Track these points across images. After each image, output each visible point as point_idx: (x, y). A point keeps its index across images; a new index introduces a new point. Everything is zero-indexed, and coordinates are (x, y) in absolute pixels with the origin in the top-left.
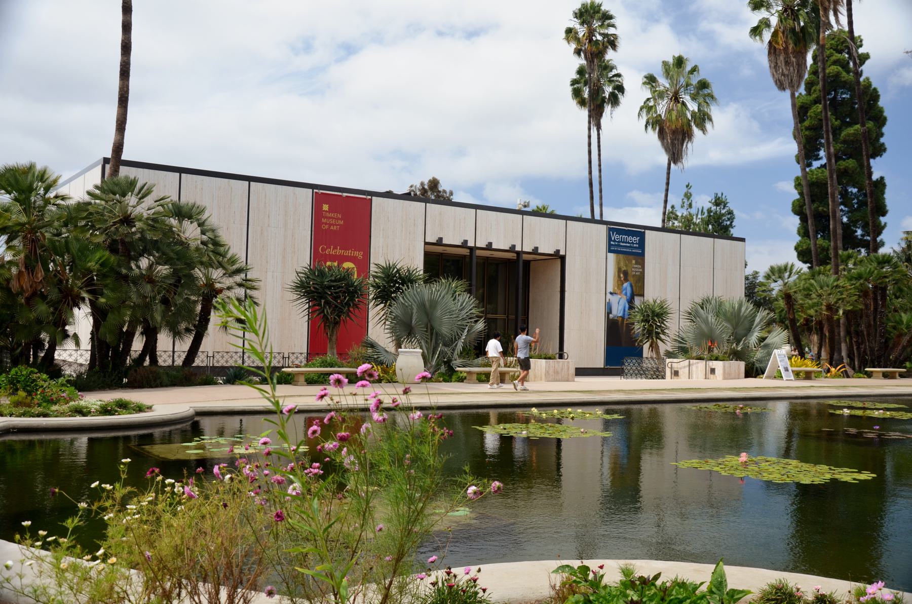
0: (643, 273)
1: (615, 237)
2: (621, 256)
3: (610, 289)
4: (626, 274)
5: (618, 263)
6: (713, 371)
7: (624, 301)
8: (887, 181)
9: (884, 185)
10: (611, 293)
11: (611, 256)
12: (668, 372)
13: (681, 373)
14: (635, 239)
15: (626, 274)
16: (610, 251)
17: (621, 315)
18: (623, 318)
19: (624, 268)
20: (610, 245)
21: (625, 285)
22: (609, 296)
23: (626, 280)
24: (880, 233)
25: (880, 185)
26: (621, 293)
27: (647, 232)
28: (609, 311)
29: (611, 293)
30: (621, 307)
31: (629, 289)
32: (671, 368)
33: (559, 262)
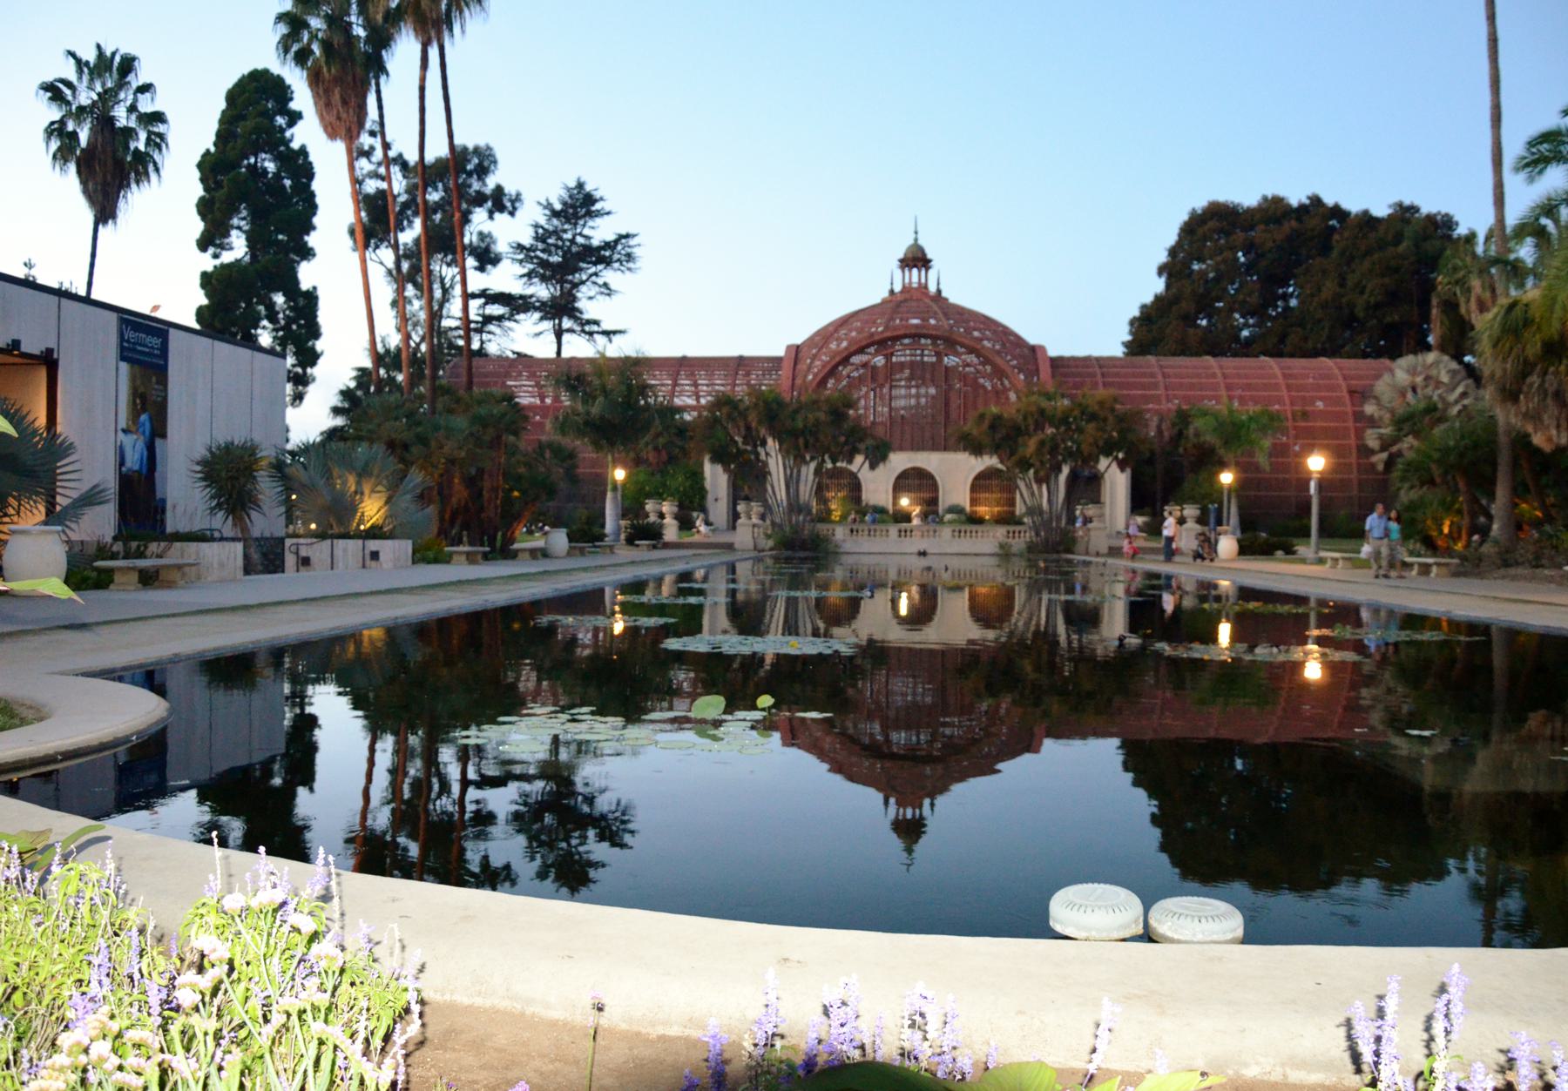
0: (165, 399)
1: (130, 334)
2: (136, 367)
3: (123, 424)
4: (143, 398)
5: (133, 379)
6: (375, 555)
7: (141, 445)
8: (320, 293)
9: (316, 298)
10: (124, 431)
11: (124, 366)
12: (290, 560)
13: (314, 560)
14: (155, 341)
15: (143, 398)
16: (123, 358)
17: (136, 467)
18: (139, 472)
19: (141, 390)
20: (122, 349)
21: (144, 417)
22: (121, 435)
23: (144, 410)
24: (313, 364)
25: (311, 298)
26: (136, 432)
27: (172, 331)
28: (122, 463)
29: (124, 431)
30: (137, 456)
31: (148, 425)
32: (297, 553)
33: (42, 374)
